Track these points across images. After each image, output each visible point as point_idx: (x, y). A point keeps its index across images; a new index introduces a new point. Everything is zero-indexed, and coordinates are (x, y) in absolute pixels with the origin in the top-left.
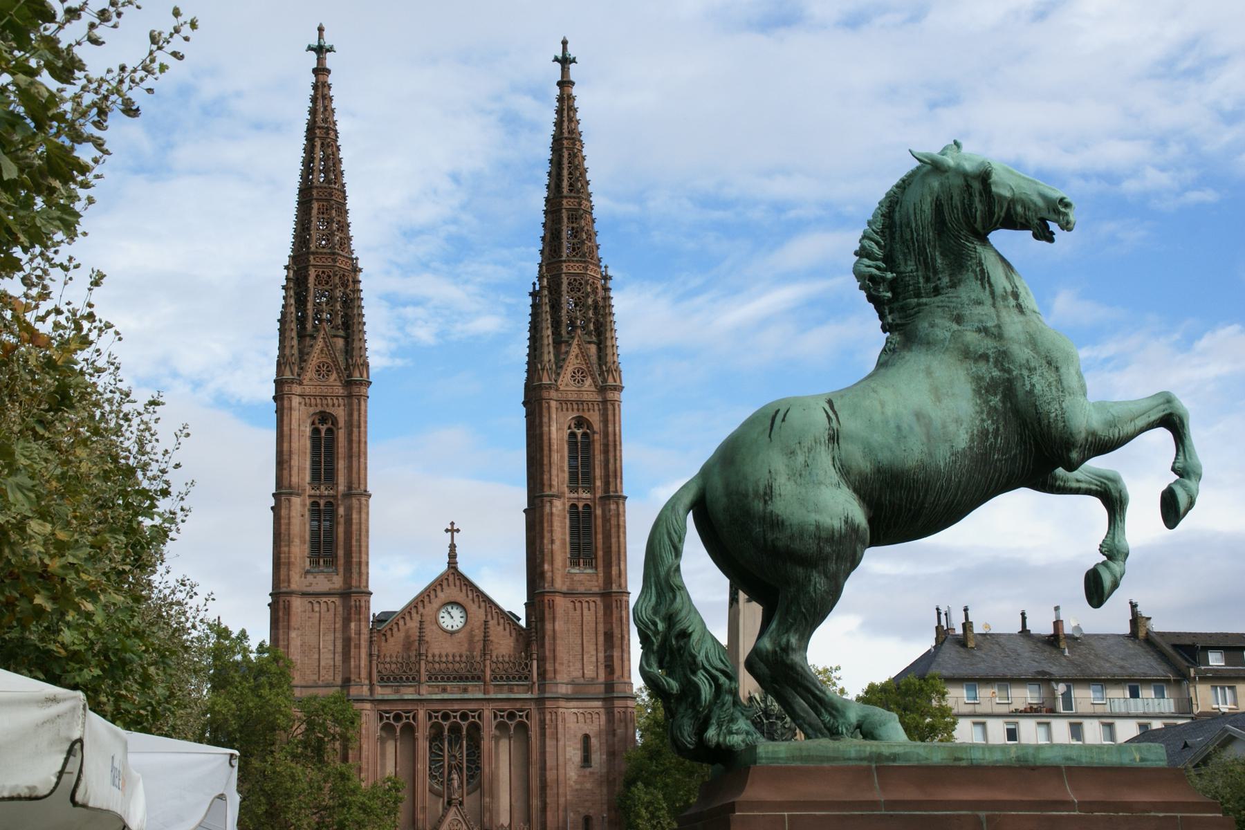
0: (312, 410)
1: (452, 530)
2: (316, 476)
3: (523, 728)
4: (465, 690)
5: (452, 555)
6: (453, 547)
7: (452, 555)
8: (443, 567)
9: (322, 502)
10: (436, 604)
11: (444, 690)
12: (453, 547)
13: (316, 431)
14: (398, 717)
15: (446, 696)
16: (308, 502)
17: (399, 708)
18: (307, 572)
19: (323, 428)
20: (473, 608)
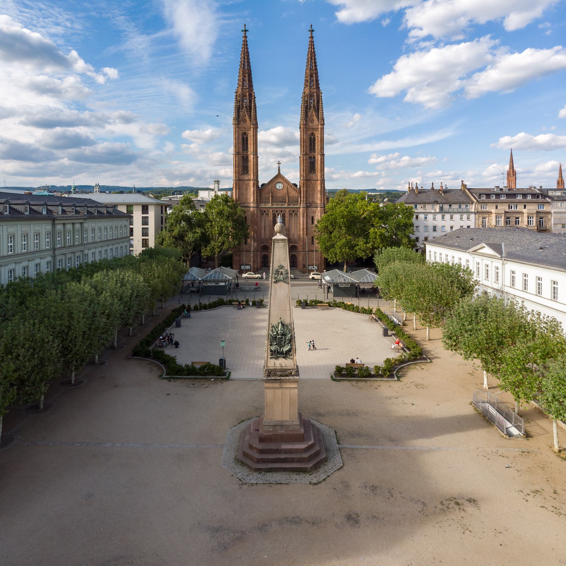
0: (242, 132)
1: (279, 163)
2: (243, 150)
3: (296, 214)
4: (282, 205)
5: (279, 170)
6: (279, 168)
7: (279, 170)
8: (277, 173)
9: (245, 156)
10: (275, 183)
11: (277, 205)
12: (279, 168)
13: (243, 137)
14: (265, 211)
15: (277, 206)
16: (242, 156)
17: (264, 209)
18: (242, 174)
19: (245, 136)
20: (285, 184)
